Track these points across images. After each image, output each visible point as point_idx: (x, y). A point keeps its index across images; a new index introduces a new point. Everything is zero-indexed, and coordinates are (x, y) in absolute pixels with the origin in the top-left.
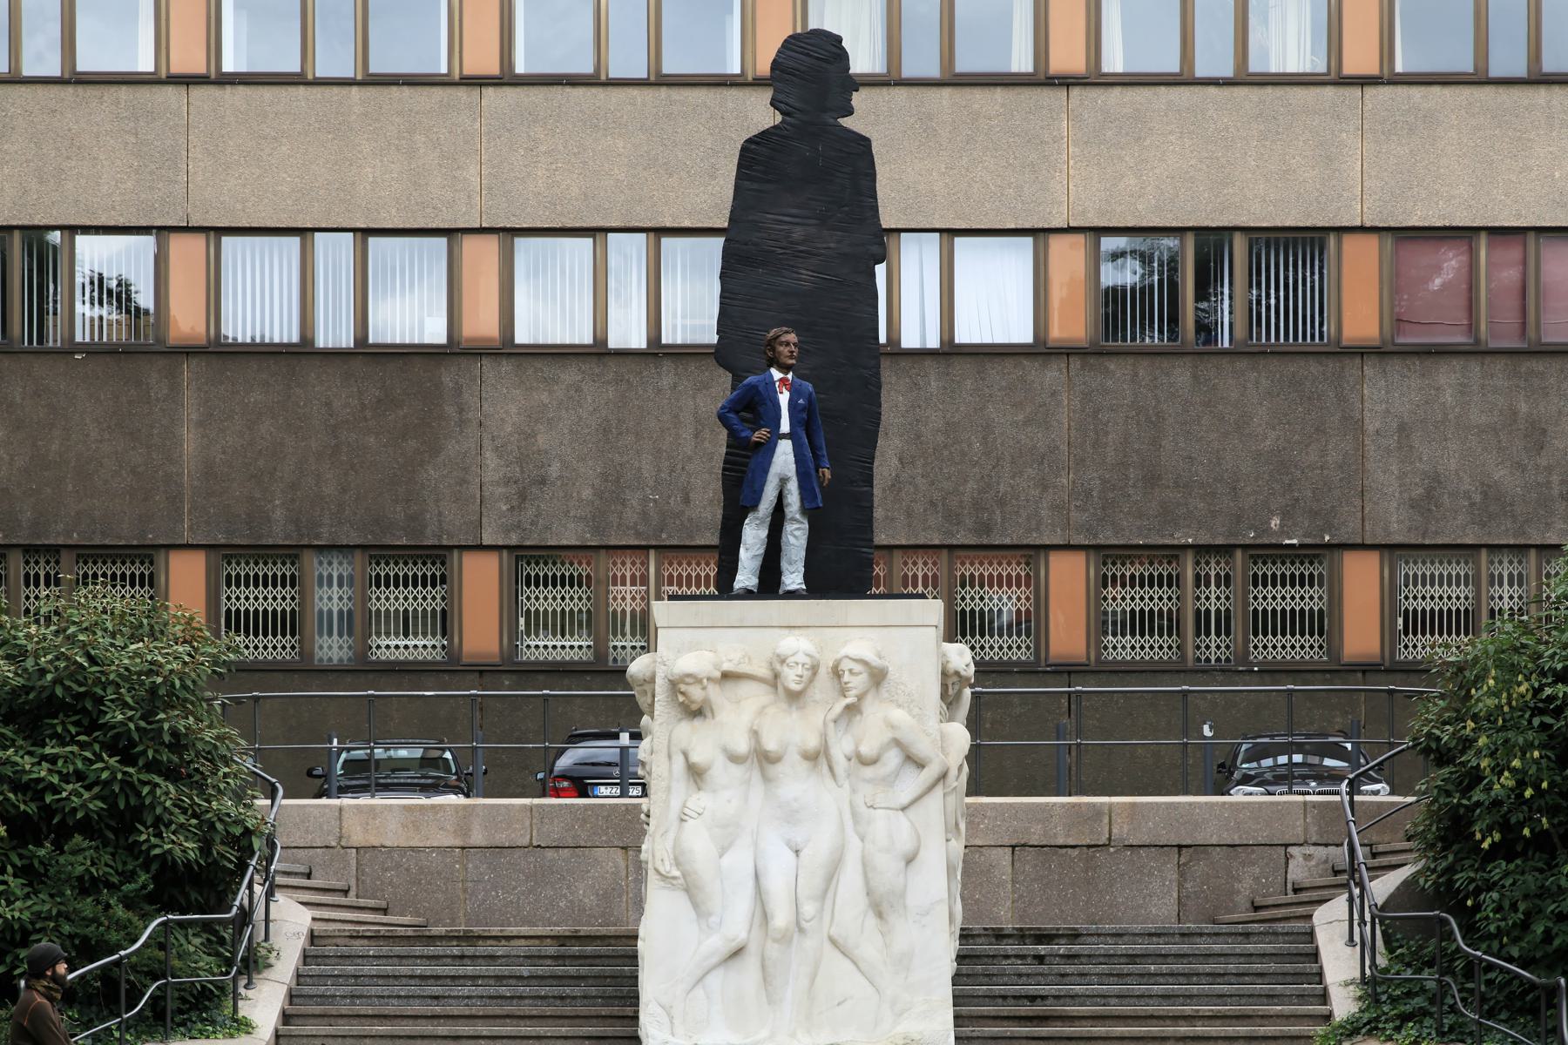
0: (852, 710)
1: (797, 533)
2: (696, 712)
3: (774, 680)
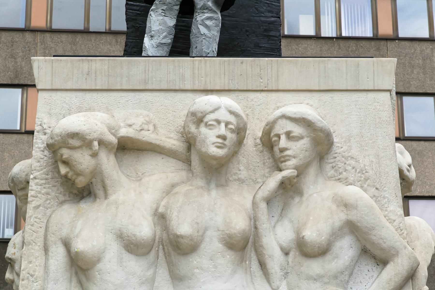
0: (289, 189)
1: (208, 23)
2: (81, 190)
3: (188, 152)
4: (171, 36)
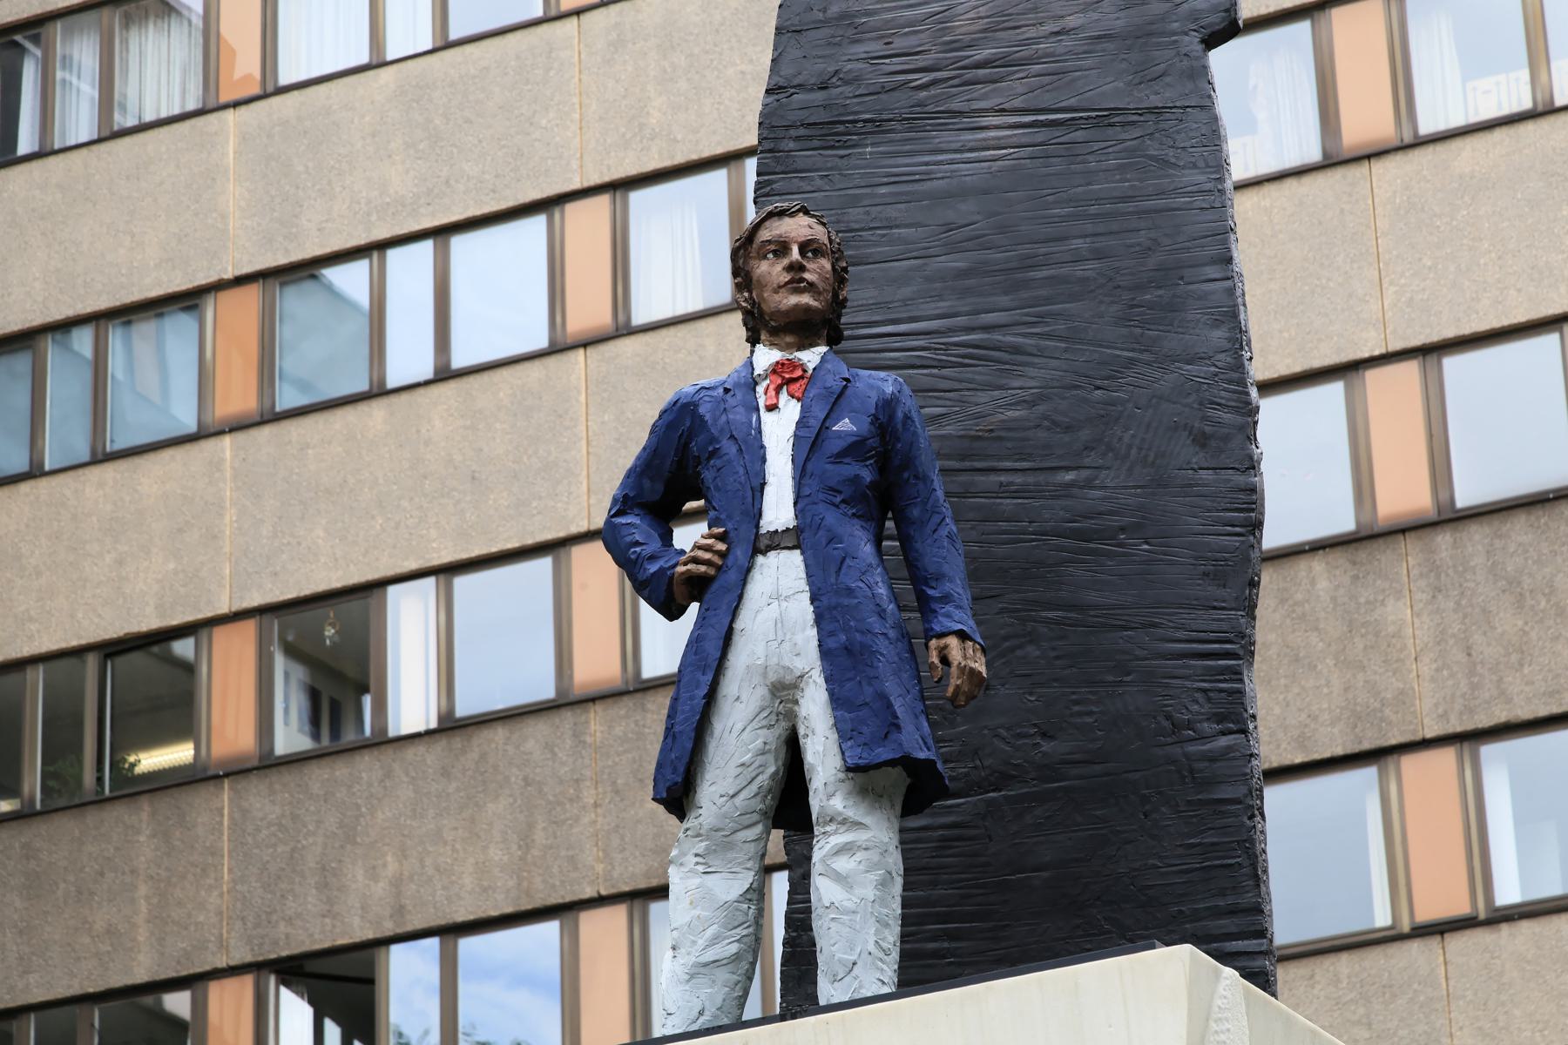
1: (843, 864)
4: (738, 930)
